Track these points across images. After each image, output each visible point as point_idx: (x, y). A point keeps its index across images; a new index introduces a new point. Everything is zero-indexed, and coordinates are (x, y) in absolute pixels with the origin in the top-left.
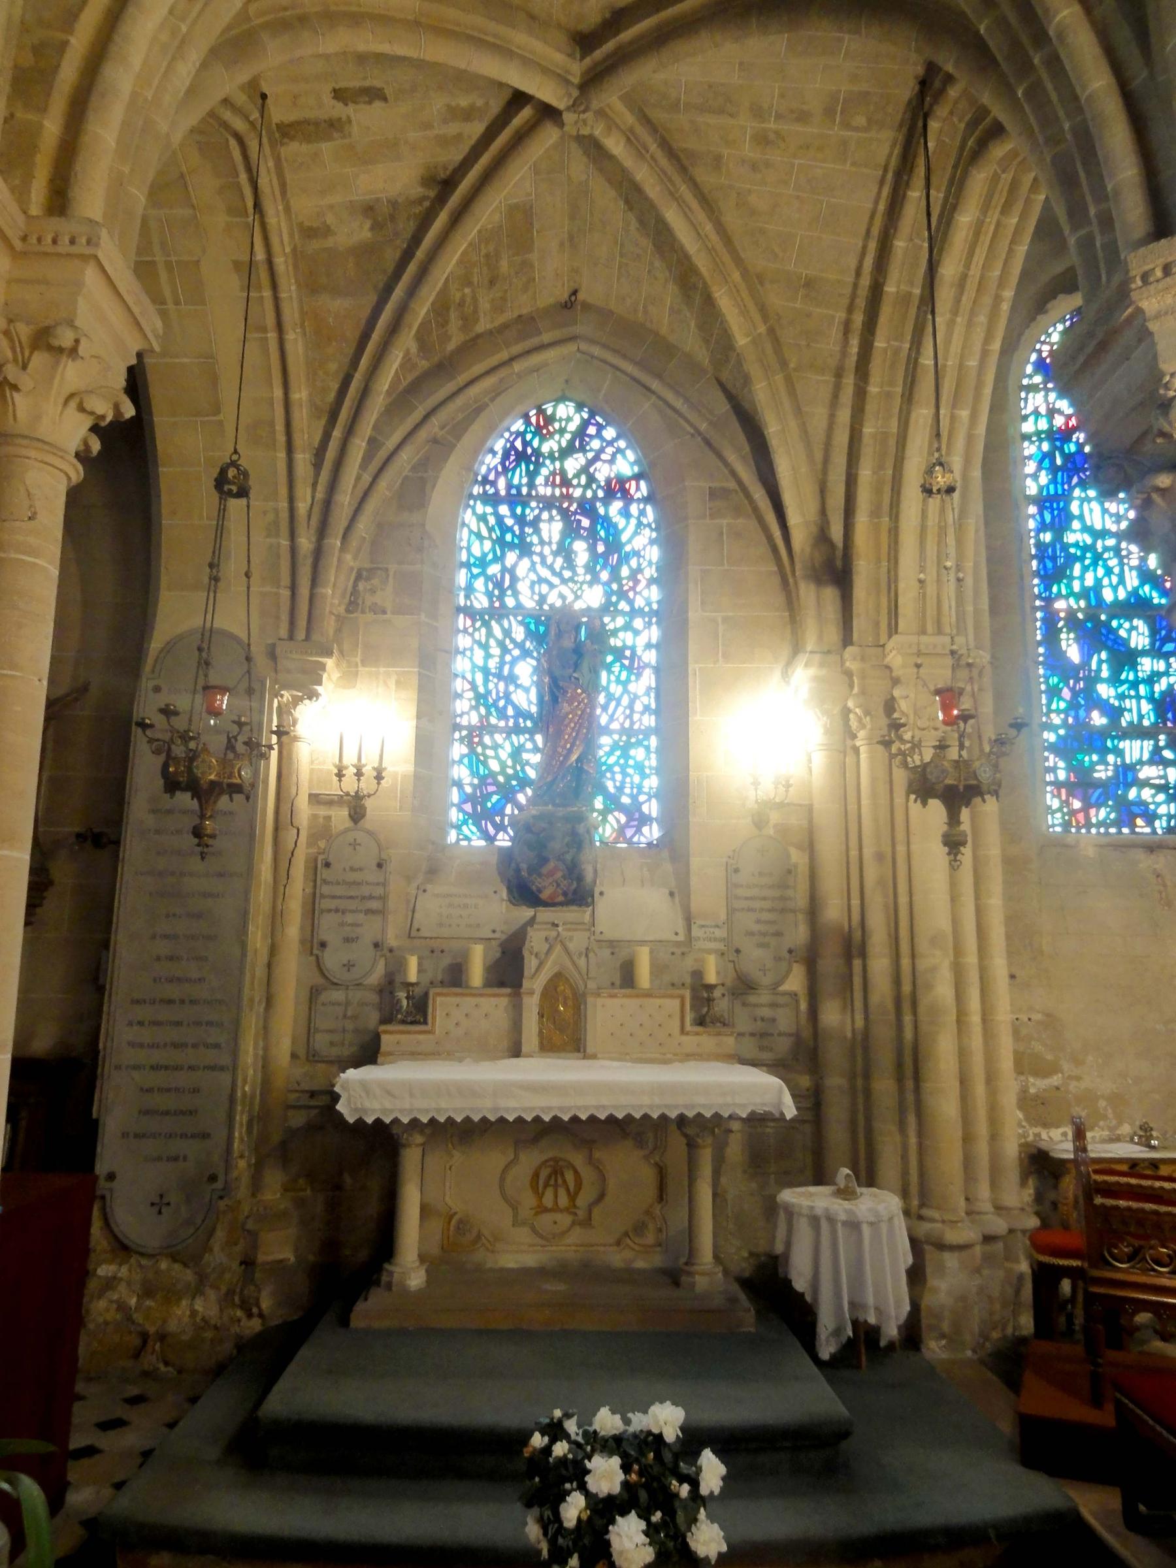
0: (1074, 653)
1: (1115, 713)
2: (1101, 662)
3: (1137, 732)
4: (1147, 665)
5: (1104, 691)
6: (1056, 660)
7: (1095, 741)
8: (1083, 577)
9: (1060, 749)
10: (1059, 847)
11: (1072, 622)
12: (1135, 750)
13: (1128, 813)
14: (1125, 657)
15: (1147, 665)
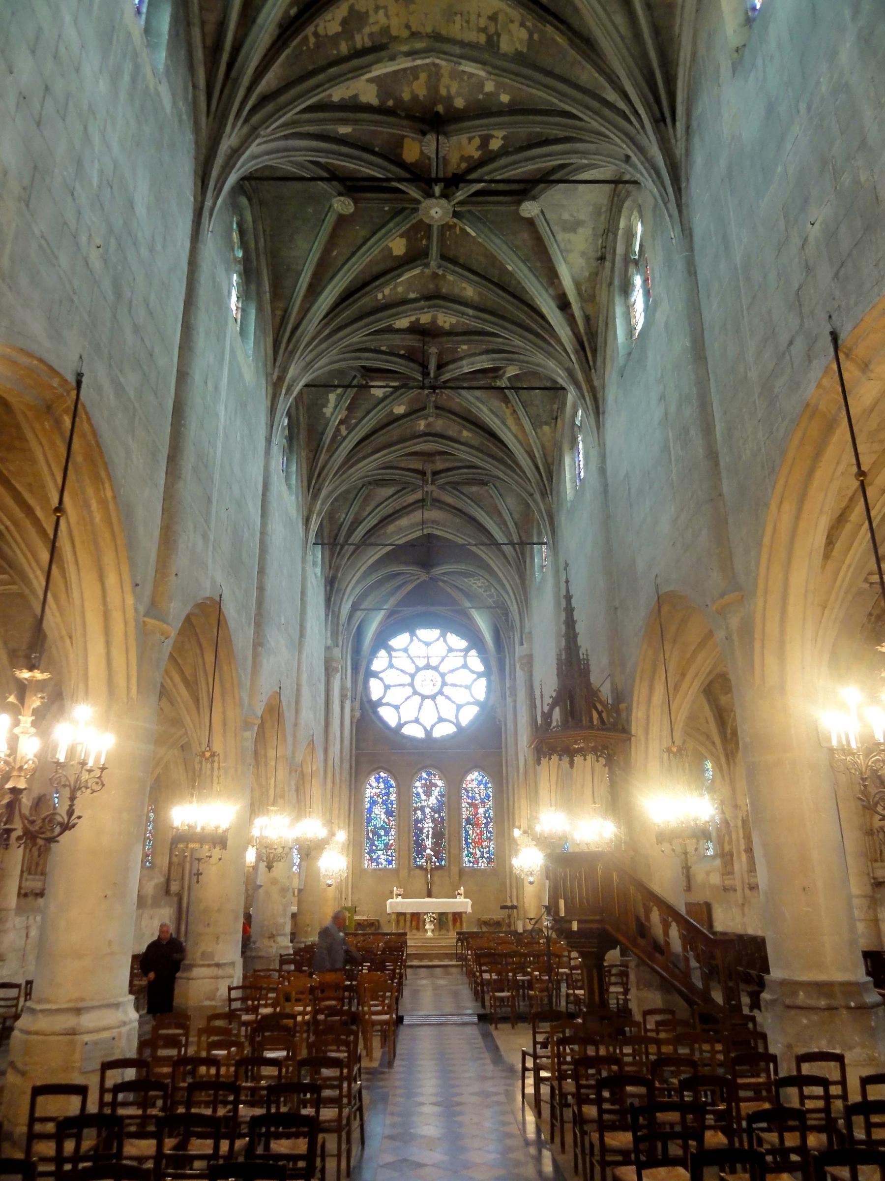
0: (371, 836)
1: (377, 846)
2: (376, 838)
3: (380, 850)
4: (383, 838)
5: (376, 843)
6: (368, 838)
7: (374, 852)
8: (373, 822)
9: (368, 853)
10: (365, 870)
11: (371, 831)
12: (380, 853)
13: (378, 864)
14: (380, 836)
15: (383, 838)
